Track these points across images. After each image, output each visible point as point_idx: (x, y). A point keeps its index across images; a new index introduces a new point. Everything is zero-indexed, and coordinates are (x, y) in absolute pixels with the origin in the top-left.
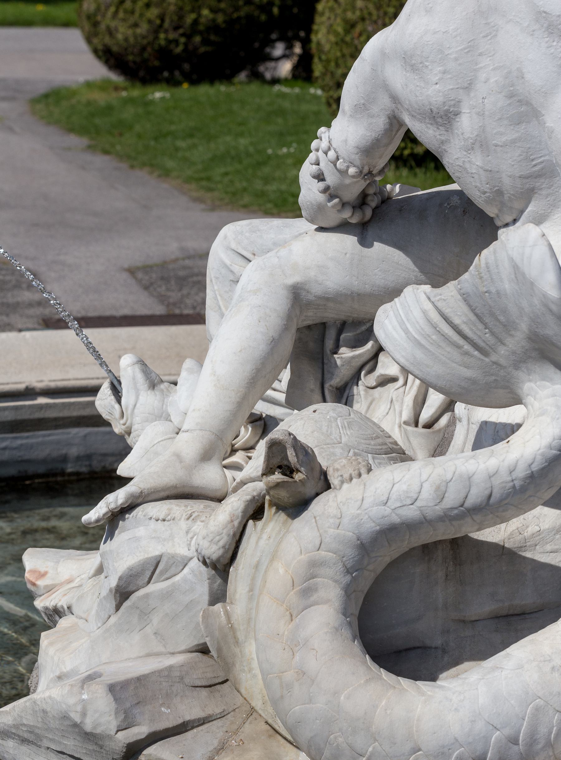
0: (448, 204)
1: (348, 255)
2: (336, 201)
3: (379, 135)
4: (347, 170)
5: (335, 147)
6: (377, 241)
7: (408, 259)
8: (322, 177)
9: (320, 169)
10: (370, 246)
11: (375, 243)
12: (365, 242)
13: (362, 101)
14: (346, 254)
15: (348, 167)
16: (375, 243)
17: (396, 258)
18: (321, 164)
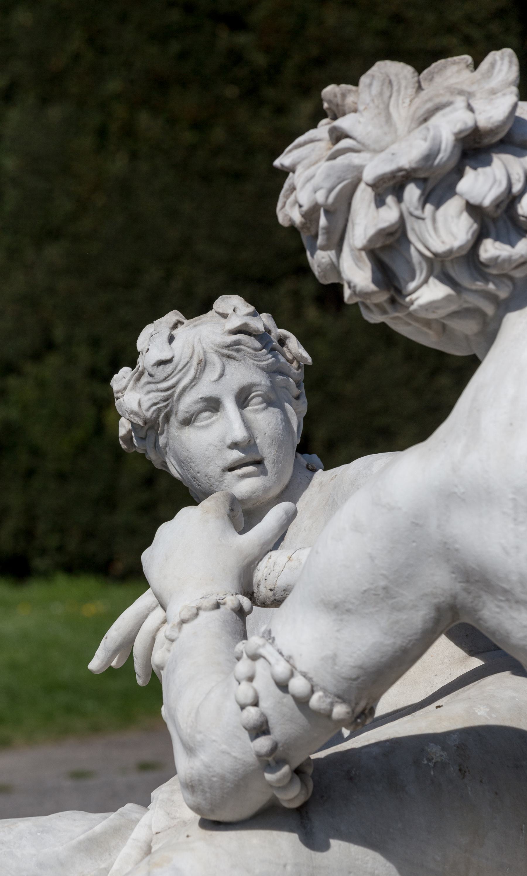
0: (430, 760)
1: (289, 868)
2: (286, 769)
3: (410, 641)
4: (331, 711)
5: (304, 669)
6: (334, 838)
7: (389, 864)
8: (264, 728)
9: (263, 715)
10: (324, 847)
11: (333, 842)
12: (314, 841)
13: (383, 583)
14: (285, 866)
15: (332, 705)
16: (333, 842)
17: (369, 865)
18: (262, 704)
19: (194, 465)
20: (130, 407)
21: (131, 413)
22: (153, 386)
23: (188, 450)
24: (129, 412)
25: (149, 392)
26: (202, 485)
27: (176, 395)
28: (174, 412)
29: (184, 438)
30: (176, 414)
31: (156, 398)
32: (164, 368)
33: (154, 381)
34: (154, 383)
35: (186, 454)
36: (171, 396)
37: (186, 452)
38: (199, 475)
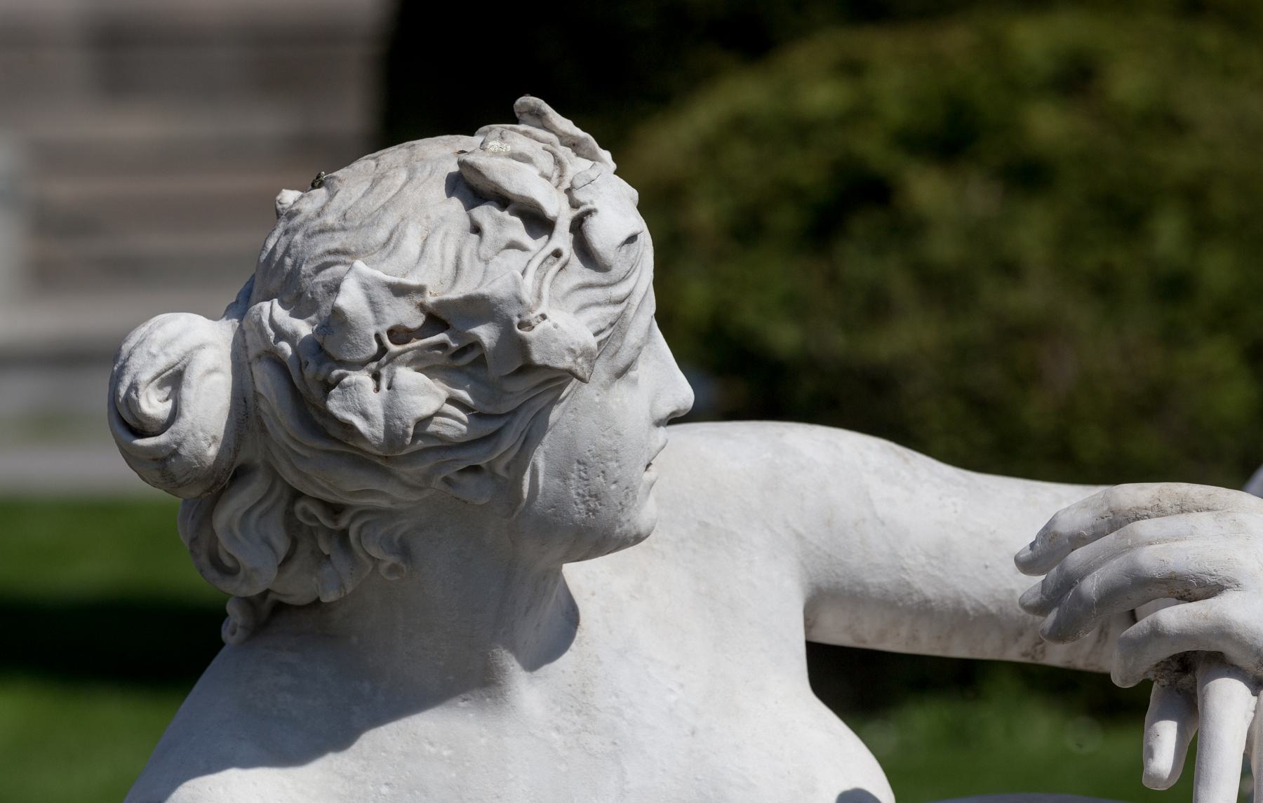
19: (615, 465)
20: (582, 341)
21: (581, 355)
22: (598, 294)
23: (618, 433)
24: (579, 352)
25: (584, 307)
26: (603, 510)
27: (631, 313)
28: (611, 350)
29: (614, 407)
30: (616, 352)
31: (605, 319)
32: (628, 252)
33: (606, 281)
34: (602, 286)
35: (610, 442)
36: (622, 315)
37: (611, 437)
38: (613, 487)
